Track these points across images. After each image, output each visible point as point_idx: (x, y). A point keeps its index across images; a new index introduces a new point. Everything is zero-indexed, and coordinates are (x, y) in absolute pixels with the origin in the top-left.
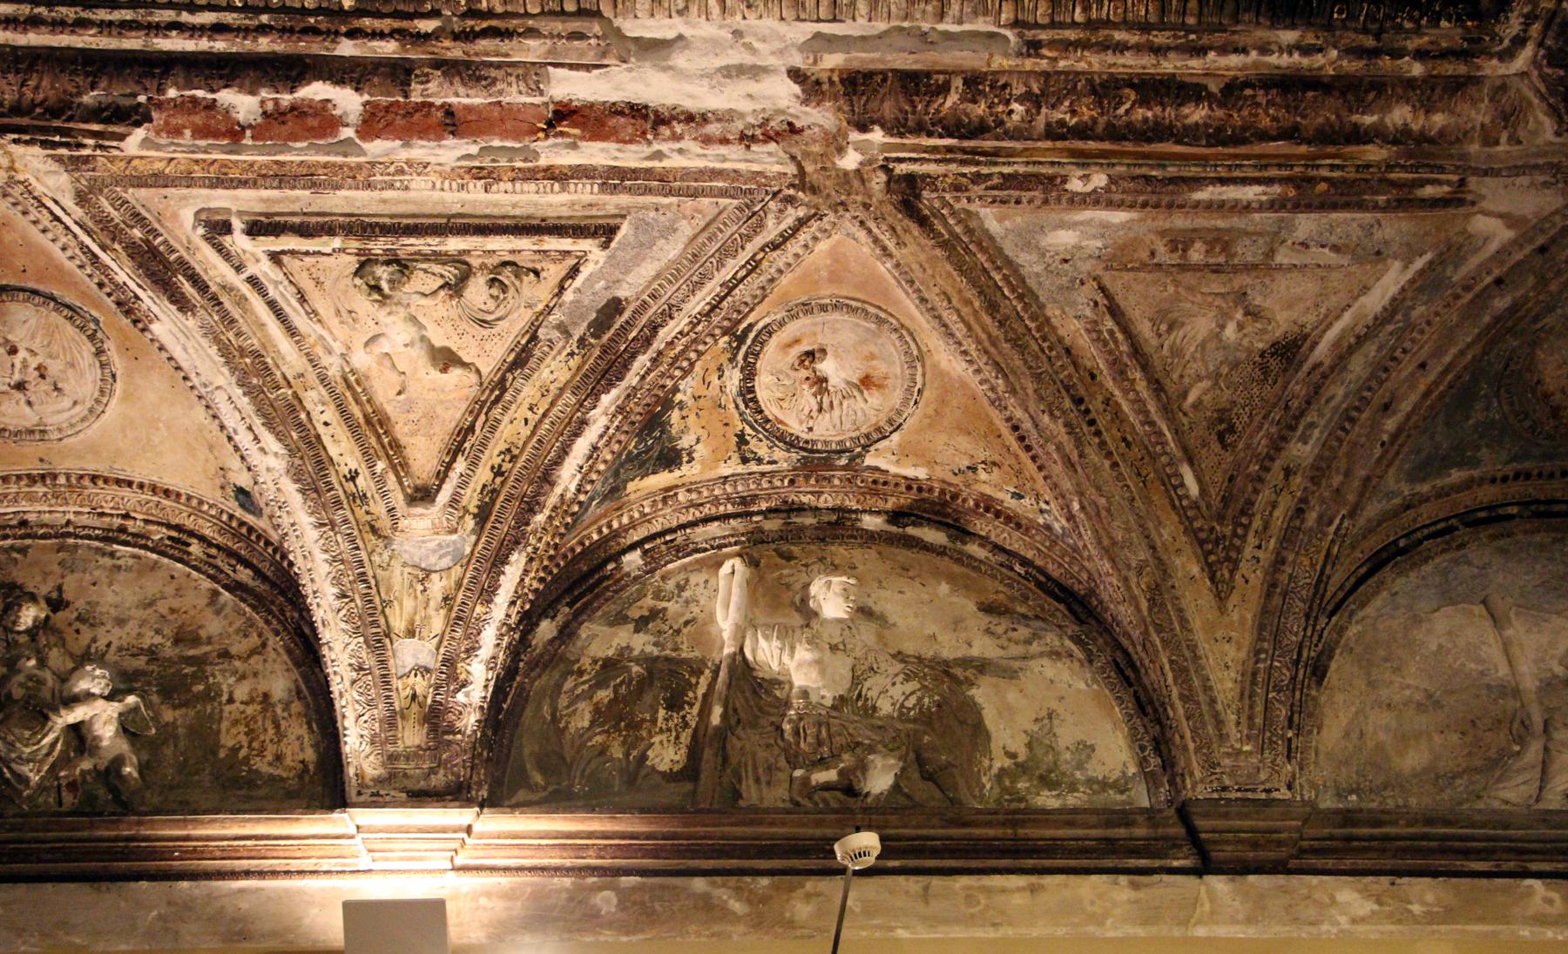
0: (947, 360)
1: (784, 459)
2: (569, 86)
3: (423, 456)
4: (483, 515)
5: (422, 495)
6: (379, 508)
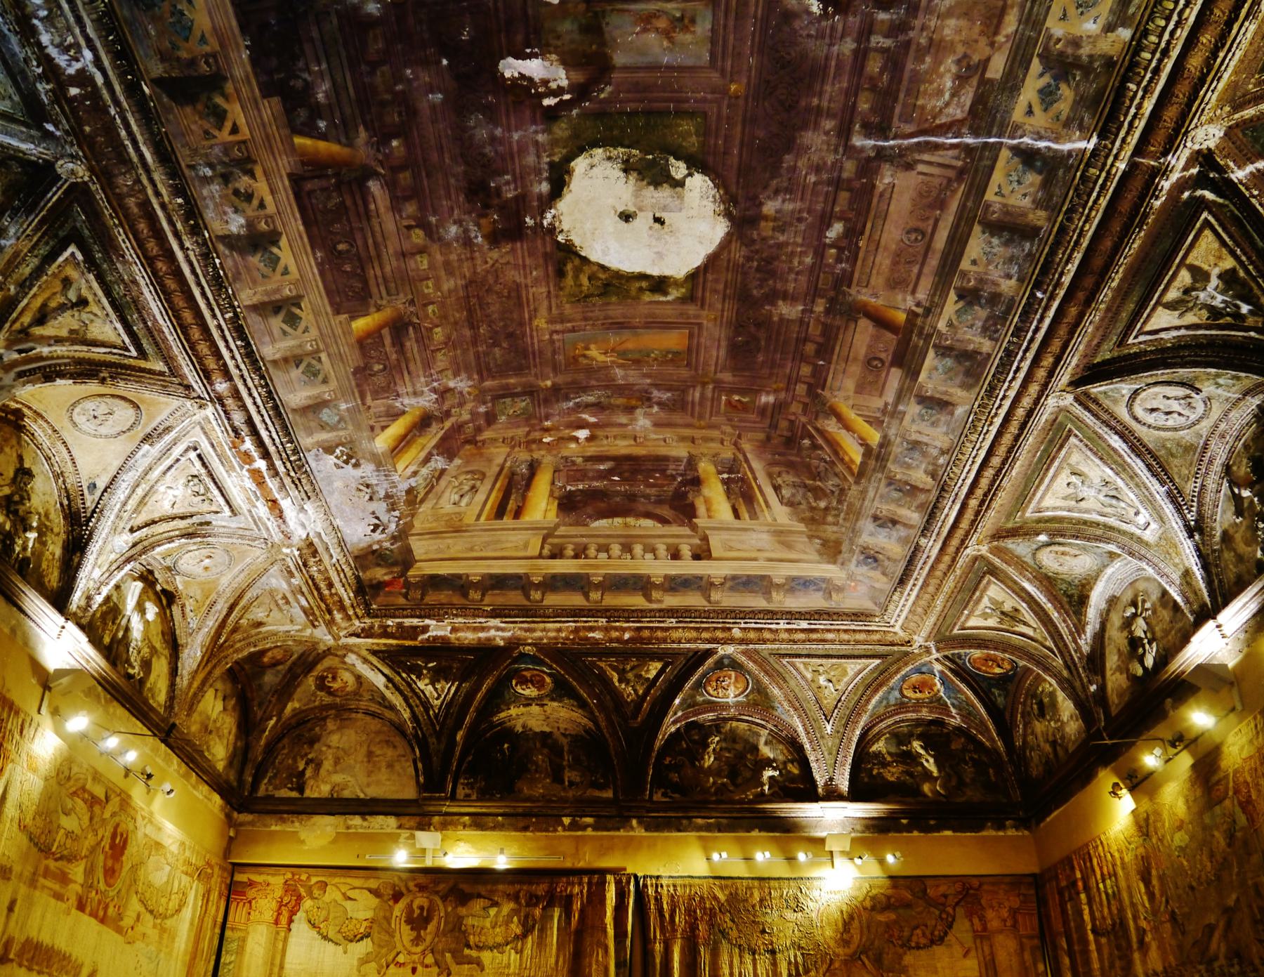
0: (224, 581)
1: (169, 562)
2: (285, 504)
4: (134, 545)
6: (122, 525)
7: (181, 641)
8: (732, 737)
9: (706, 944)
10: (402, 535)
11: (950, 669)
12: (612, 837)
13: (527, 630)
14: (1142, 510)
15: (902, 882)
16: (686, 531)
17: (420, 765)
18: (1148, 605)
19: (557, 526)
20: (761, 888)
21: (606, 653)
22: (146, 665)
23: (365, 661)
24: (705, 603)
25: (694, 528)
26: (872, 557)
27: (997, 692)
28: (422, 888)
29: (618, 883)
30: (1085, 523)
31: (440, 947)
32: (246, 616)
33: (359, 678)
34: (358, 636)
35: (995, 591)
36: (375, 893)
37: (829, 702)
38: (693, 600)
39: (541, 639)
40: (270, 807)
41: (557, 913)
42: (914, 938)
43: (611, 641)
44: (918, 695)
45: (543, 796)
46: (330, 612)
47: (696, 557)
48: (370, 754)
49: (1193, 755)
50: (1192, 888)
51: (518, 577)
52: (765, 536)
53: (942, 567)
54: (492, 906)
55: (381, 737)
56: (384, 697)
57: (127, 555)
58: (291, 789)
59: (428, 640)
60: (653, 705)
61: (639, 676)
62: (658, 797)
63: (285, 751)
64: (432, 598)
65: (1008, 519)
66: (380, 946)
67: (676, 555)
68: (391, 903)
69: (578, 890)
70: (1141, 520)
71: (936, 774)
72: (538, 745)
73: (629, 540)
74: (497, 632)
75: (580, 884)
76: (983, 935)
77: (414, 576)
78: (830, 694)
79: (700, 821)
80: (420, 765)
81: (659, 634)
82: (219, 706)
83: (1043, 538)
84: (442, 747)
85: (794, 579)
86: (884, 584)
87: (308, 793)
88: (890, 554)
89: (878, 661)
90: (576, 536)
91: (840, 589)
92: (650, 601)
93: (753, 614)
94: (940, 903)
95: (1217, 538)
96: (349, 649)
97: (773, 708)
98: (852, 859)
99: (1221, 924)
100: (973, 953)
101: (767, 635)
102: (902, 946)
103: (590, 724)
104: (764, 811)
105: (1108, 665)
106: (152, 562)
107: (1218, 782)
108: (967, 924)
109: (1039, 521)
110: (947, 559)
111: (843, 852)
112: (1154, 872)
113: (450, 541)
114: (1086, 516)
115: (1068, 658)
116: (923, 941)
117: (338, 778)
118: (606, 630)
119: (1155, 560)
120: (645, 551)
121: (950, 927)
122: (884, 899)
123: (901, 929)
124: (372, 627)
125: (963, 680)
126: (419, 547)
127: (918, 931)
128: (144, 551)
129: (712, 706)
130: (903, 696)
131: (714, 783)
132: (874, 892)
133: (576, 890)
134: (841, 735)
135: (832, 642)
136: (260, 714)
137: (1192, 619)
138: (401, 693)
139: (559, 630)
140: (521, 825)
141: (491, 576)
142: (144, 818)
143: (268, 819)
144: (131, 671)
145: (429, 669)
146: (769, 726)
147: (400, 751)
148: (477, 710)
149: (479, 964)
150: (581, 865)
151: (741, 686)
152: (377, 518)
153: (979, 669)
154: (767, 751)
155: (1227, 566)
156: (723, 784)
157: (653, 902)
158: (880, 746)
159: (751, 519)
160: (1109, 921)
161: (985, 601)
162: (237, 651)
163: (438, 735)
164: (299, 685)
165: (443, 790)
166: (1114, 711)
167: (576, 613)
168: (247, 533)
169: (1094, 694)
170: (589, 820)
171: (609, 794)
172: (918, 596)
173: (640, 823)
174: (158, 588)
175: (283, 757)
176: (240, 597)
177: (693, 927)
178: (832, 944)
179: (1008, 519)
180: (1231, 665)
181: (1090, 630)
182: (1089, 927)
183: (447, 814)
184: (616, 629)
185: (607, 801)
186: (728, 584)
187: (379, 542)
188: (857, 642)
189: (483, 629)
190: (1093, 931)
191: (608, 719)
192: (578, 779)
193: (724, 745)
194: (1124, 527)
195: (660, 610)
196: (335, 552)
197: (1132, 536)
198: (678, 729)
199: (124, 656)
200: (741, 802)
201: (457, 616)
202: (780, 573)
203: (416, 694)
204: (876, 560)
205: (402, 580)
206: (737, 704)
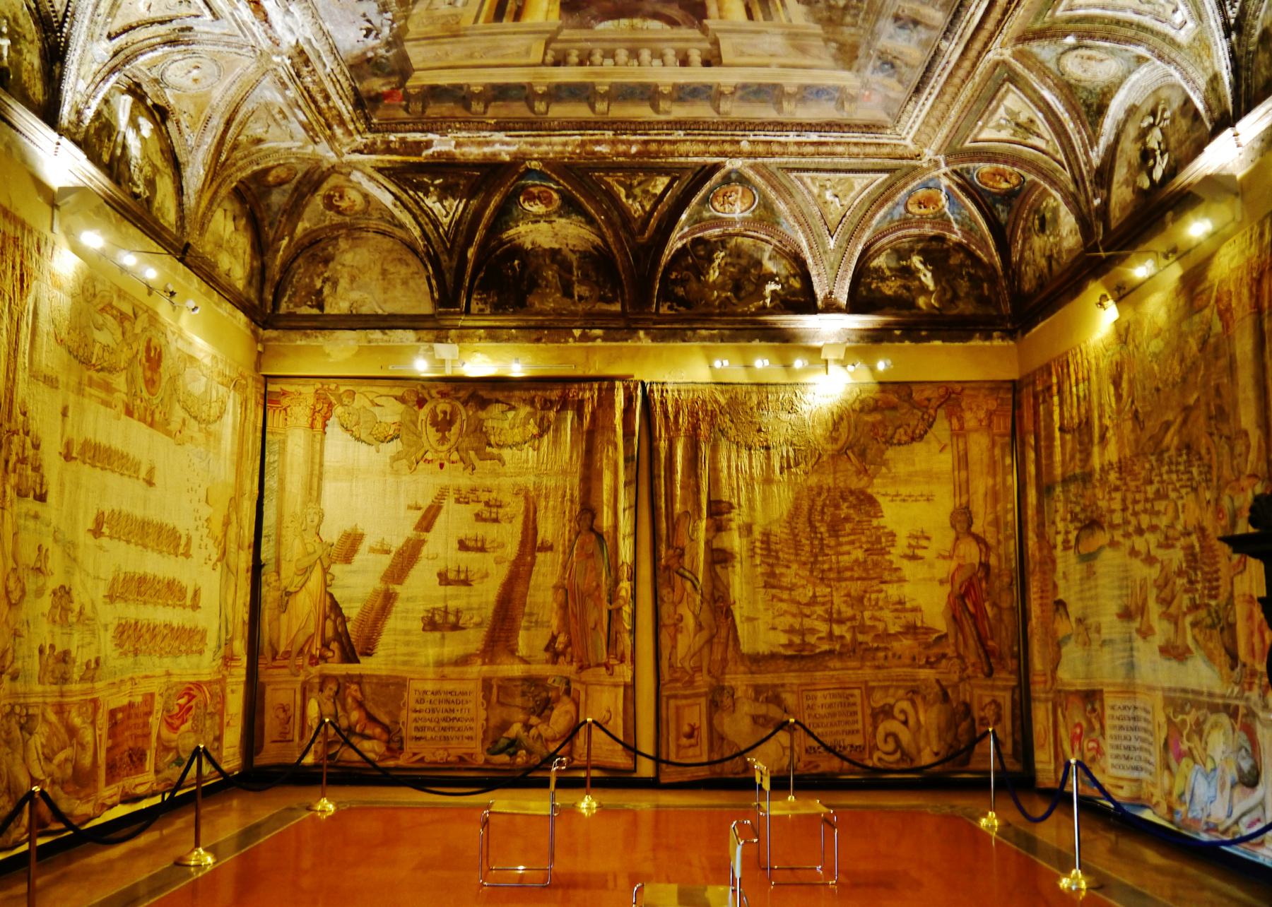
0: (217, 94)
1: (155, 73)
3: (117, 25)
4: (116, 54)
5: (110, 37)
6: (98, 31)
7: (182, 159)
8: (738, 253)
9: (707, 440)
10: (396, 40)
11: (958, 185)
12: (620, 348)
13: (532, 144)
14: (1181, 7)
15: (890, 387)
16: (695, 33)
17: (434, 282)
18: (1167, 114)
19: (560, 29)
20: (759, 392)
21: (613, 168)
22: (151, 184)
23: (371, 178)
24: (714, 114)
25: (704, 30)
26: (889, 63)
27: (1000, 207)
28: (443, 395)
29: (626, 388)
30: (1118, 22)
31: (464, 445)
32: (245, 132)
33: (366, 196)
34: (361, 152)
35: (1013, 101)
36: (402, 400)
37: (833, 217)
38: (701, 111)
39: (547, 153)
40: (293, 324)
41: (570, 415)
42: (897, 436)
43: (618, 155)
44: (923, 211)
45: (554, 310)
46: (330, 128)
47: (706, 63)
48: (384, 272)
49: (1183, 266)
50: (1158, 390)
51: (521, 87)
52: (779, 40)
53: (961, 73)
54: (510, 409)
55: (395, 255)
56: (393, 216)
57: (111, 64)
58: (311, 307)
59: (432, 156)
60: (660, 221)
61: (646, 192)
62: (664, 309)
63: (302, 270)
64: (434, 110)
65: (1036, 19)
66: (409, 446)
67: (685, 62)
68: (416, 408)
69: (589, 395)
70: (1178, 18)
71: (931, 286)
72: (548, 261)
73: (636, 45)
74: (503, 146)
75: (591, 389)
76: (960, 433)
77: (414, 87)
78: (835, 208)
79: (704, 332)
80: (434, 282)
81: (667, 147)
82: (230, 226)
83: (1071, 40)
84: (454, 264)
85: (806, 87)
86: (898, 92)
87: (327, 310)
88: (908, 59)
89: (885, 176)
90: (580, 41)
91: (853, 99)
92: (657, 111)
93: (763, 126)
94: (923, 406)
95: (1255, 39)
96: (353, 166)
97: (778, 223)
98: (845, 366)
99: (1179, 420)
100: (949, 449)
101: (776, 148)
102: (886, 443)
103: (598, 241)
104: (765, 323)
105: (1116, 179)
106: (138, 73)
107: (1203, 292)
108: (946, 424)
109: (1070, 20)
110: (967, 64)
111: (837, 361)
112: (1125, 376)
113: (448, 47)
114: (1120, 15)
115: (1076, 172)
116: (904, 438)
117: (355, 295)
118: (613, 143)
119: (1184, 64)
120: (653, 56)
121: (930, 426)
122: (872, 402)
123: (886, 428)
124: (374, 143)
125: (969, 195)
126: (416, 54)
127: (901, 431)
128: (127, 61)
129: (718, 222)
130: (908, 211)
131: (718, 297)
132: (863, 396)
133: (587, 395)
134: (843, 251)
135: (841, 155)
136: (271, 234)
137: (1209, 127)
138: (410, 211)
139: (565, 144)
140: (534, 336)
141: (495, 87)
142: (174, 333)
143: (293, 334)
144: (135, 190)
145: (436, 186)
146: (774, 241)
147: (413, 269)
148: (486, 227)
149: (500, 459)
150: (592, 372)
151: (748, 201)
152: (369, 21)
153: (986, 184)
154: (770, 266)
155: (1258, 69)
156: (727, 298)
157: (658, 405)
158: (880, 261)
159: (765, 19)
160: (1076, 420)
161: (1001, 111)
162: (241, 169)
163: (450, 252)
164: (307, 204)
165: (457, 304)
166: (1114, 224)
167: (582, 125)
168: (233, 40)
169: (1097, 209)
170: (598, 332)
171: (617, 307)
172: (932, 106)
173: (647, 334)
174: (149, 102)
175: (300, 275)
176: (235, 111)
177: (695, 427)
178: (821, 441)
179: (1036, 19)
180: (1239, 175)
181: (1103, 142)
182: (1057, 425)
183: (463, 328)
184: (623, 142)
185: (615, 315)
186: (739, 93)
187: (373, 49)
188: (867, 156)
189: (488, 143)
190: (1062, 429)
191: (616, 235)
192: (587, 294)
193: (729, 260)
194: (1159, 26)
195: (668, 122)
196: (328, 59)
197: (1165, 37)
198: (684, 246)
199: (127, 175)
200: (744, 314)
201: (460, 129)
202: (793, 80)
203: (424, 212)
204: (893, 66)
205: (401, 91)
206: (744, 220)
